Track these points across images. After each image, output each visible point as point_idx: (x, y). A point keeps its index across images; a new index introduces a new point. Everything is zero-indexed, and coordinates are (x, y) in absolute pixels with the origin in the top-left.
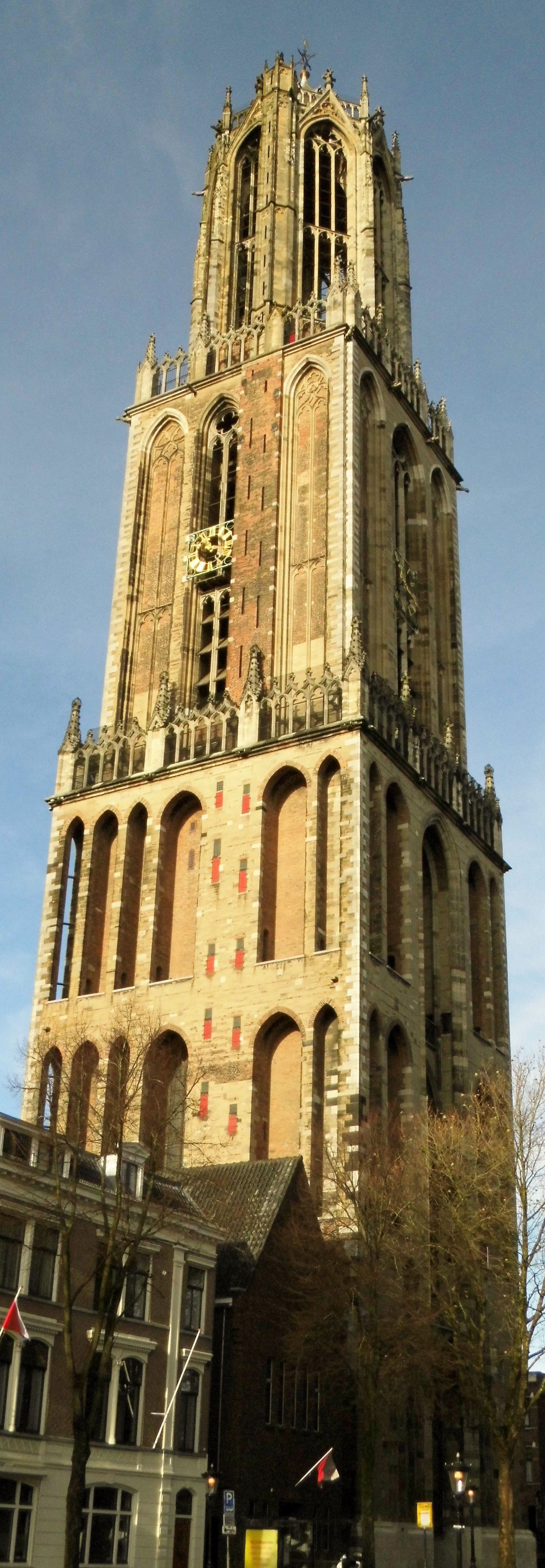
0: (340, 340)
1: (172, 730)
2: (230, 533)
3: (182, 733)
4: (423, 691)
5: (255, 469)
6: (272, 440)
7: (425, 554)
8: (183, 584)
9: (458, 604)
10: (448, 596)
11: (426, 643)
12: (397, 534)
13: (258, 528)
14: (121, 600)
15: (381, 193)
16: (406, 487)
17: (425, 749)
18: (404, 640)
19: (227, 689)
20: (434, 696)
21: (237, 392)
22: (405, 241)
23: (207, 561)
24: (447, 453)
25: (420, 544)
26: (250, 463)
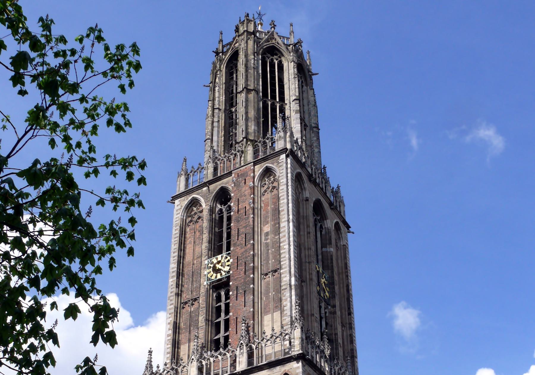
0: (283, 156)
1: (201, 362)
2: (229, 258)
3: (207, 364)
4: (334, 338)
5: (241, 224)
6: (249, 209)
7: (332, 266)
8: (205, 286)
9: (350, 292)
10: (345, 288)
11: (335, 313)
12: (317, 256)
13: (243, 255)
14: (172, 296)
15: (302, 81)
16: (321, 232)
17: (337, 368)
18: (323, 312)
19: (230, 340)
20: (340, 341)
21: (230, 185)
22: (315, 105)
23: (217, 273)
24: (342, 214)
25: (329, 261)
26: (238, 221)
